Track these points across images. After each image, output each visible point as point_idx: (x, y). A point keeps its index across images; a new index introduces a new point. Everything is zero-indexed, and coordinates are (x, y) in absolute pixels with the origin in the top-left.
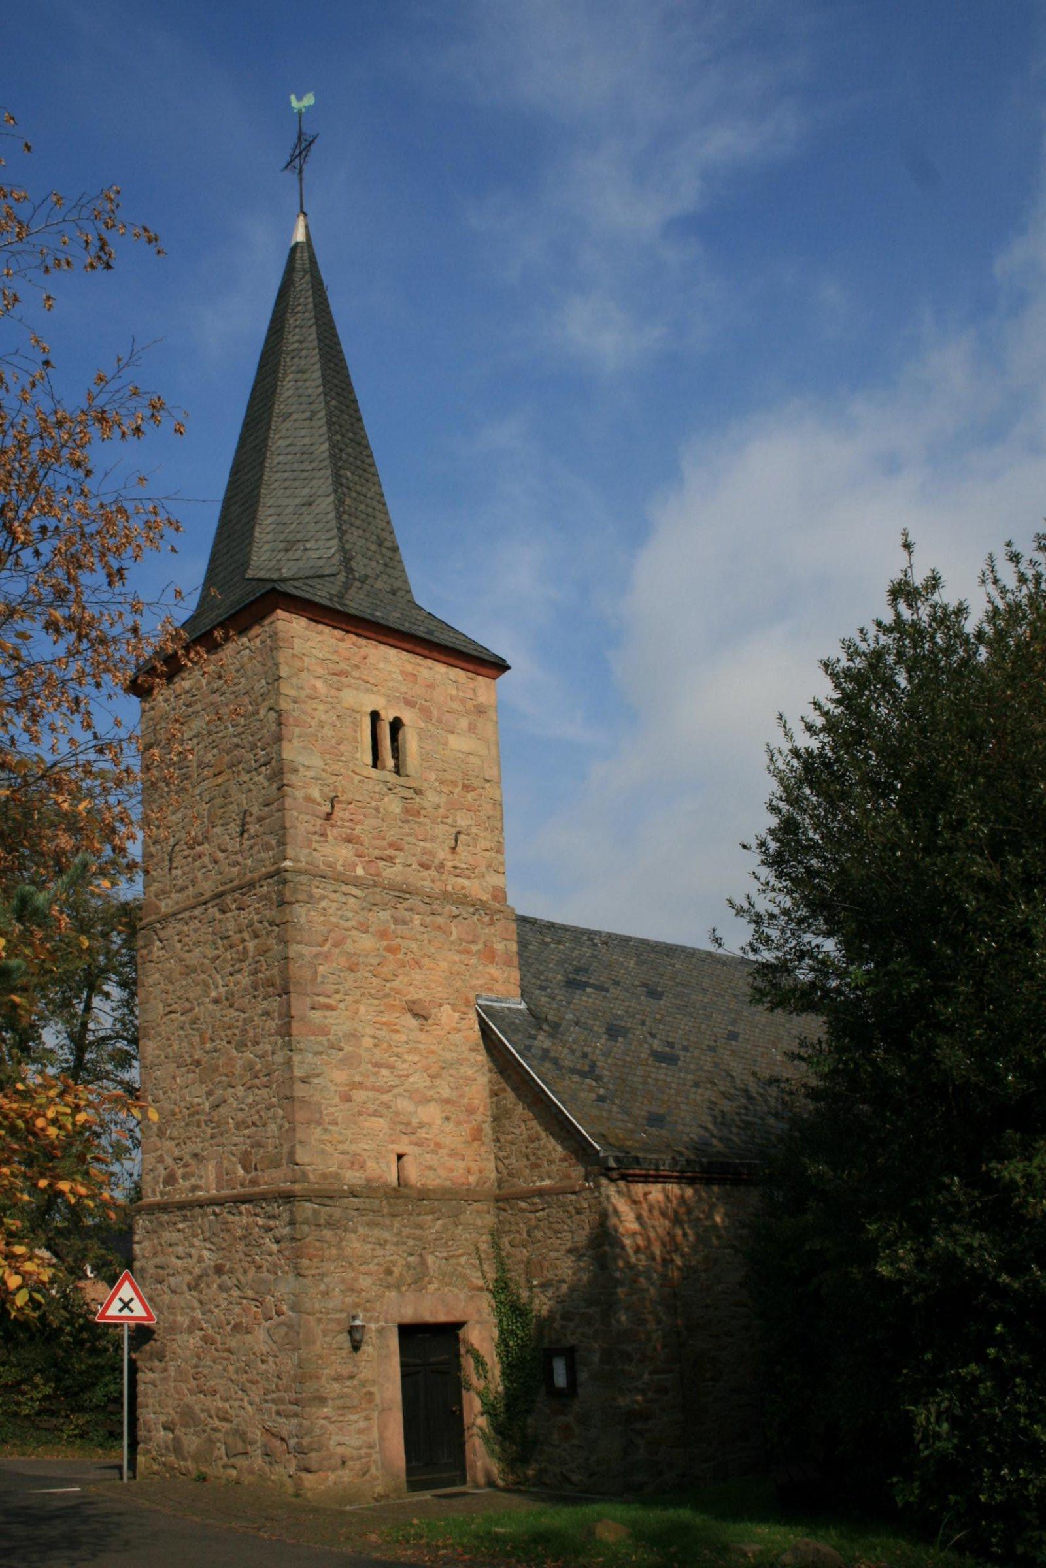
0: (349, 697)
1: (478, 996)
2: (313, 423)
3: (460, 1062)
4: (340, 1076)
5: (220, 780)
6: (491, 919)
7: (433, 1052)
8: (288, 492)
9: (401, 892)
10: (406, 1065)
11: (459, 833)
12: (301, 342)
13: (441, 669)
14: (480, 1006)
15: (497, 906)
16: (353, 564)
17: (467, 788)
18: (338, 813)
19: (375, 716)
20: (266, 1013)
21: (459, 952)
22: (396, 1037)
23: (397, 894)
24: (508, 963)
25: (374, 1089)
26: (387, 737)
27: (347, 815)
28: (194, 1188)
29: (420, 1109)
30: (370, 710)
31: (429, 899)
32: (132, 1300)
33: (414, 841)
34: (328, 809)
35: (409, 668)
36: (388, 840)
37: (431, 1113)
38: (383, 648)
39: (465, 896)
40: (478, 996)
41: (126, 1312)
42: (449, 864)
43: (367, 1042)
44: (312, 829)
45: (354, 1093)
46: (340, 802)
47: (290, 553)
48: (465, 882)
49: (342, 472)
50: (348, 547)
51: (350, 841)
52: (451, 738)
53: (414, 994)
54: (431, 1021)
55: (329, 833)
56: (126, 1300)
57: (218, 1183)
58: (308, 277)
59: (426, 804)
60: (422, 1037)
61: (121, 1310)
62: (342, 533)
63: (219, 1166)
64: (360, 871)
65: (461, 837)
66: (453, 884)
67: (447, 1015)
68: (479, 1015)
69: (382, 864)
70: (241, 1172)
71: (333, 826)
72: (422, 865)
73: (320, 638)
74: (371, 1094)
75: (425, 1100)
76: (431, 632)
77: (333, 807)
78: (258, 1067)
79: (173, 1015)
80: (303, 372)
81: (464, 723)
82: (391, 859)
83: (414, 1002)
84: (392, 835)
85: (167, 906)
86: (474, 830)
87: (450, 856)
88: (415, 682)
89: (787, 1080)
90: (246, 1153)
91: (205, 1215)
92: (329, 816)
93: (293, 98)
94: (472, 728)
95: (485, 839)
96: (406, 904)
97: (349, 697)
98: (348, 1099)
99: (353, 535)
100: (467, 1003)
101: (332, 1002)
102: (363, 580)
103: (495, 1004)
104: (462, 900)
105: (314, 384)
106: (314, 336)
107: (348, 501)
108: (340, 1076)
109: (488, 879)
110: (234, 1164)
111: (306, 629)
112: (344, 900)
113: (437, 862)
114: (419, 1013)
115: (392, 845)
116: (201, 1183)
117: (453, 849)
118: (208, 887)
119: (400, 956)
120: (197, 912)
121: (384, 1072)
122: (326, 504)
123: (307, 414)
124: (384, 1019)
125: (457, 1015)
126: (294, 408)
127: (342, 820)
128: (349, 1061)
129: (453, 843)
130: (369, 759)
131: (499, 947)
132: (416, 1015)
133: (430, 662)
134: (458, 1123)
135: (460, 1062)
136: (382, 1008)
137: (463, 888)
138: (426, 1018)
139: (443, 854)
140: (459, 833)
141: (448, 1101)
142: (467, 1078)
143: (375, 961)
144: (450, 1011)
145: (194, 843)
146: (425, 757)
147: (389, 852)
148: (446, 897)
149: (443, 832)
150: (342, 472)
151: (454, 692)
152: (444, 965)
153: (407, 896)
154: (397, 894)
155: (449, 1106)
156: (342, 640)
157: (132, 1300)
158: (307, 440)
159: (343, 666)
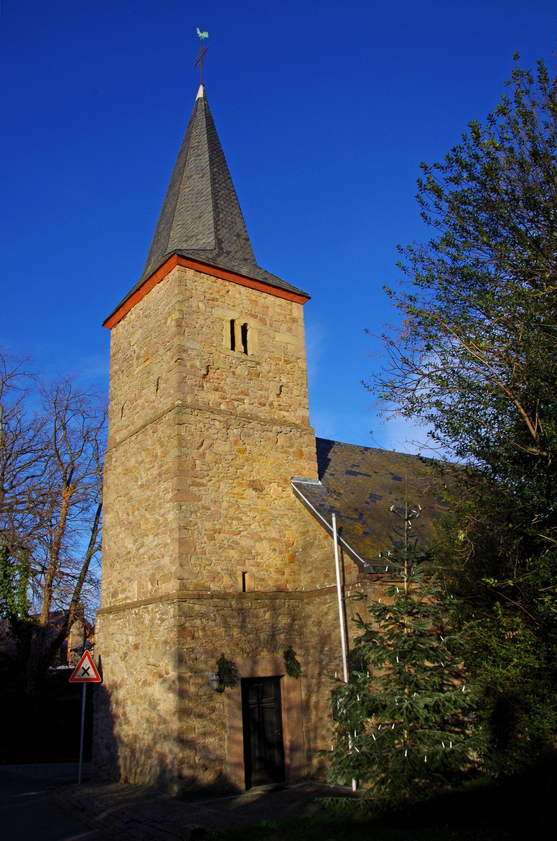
0: (218, 312)
1: (292, 478)
2: (204, 179)
3: (282, 516)
4: (208, 525)
5: (147, 363)
6: (301, 434)
7: (265, 511)
8: (189, 213)
9: (248, 418)
10: (248, 519)
11: (281, 386)
12: (199, 142)
13: (272, 298)
14: (294, 483)
15: (304, 427)
16: (223, 245)
17: (287, 362)
18: (211, 375)
19: (232, 322)
20: (166, 489)
21: (282, 453)
22: (243, 501)
23: (244, 419)
24: (310, 459)
25: (229, 532)
26: (240, 335)
27: (216, 376)
28: (127, 598)
29: (257, 544)
30: (230, 319)
31: (264, 422)
32: (89, 668)
33: (256, 390)
34: (204, 372)
35: (254, 298)
36: (240, 390)
37: (263, 547)
38: (238, 286)
39: (286, 421)
40: (292, 478)
41: (86, 676)
42: (276, 404)
43: (225, 504)
44: (194, 383)
45: (216, 535)
46: (212, 368)
47: (188, 242)
48: (284, 413)
49: (218, 201)
50: (219, 237)
51: (217, 390)
52: (277, 334)
53: (255, 476)
54: (264, 492)
55: (205, 385)
56: (86, 668)
57: (138, 595)
58: (203, 113)
59: (264, 371)
60: (259, 501)
61: (83, 675)
62: (217, 230)
63: (139, 584)
64: (223, 407)
65: (283, 389)
66: (278, 415)
67: (273, 489)
68: (294, 489)
69: (236, 403)
70: (150, 587)
71: (207, 381)
72: (260, 404)
73: (201, 281)
74: (228, 536)
75: (260, 539)
76: (266, 279)
77: (208, 371)
78: (161, 522)
79: (120, 498)
80: (199, 155)
81: (284, 327)
82: (242, 400)
83: (254, 481)
84: (242, 387)
85: (120, 437)
86: (291, 384)
87: (276, 399)
88: (257, 305)
89: (513, 133)
90: (154, 575)
91: (130, 614)
92: (205, 376)
93: (198, 30)
94: (290, 330)
95: (297, 390)
96: (250, 426)
97: (218, 312)
98: (212, 538)
99: (224, 232)
100: (286, 481)
101: (204, 481)
102: (228, 253)
103: (303, 482)
104: (284, 423)
105: (205, 161)
106: (206, 139)
107: (221, 216)
108: (208, 525)
109: (298, 411)
110: (147, 582)
111: (194, 276)
112: (212, 423)
113: (269, 402)
114: (257, 487)
115: (242, 393)
116: (129, 595)
117: (278, 395)
118: (139, 423)
119: (247, 455)
120: (133, 438)
121: (235, 522)
122: (209, 218)
123: (201, 175)
124: (235, 491)
125: (280, 488)
126: (194, 173)
127: (213, 378)
128: (214, 516)
129: (278, 392)
130: (229, 346)
131: (305, 450)
132: (255, 489)
133: (264, 295)
134: (281, 553)
135: (282, 516)
136: (235, 485)
137: (284, 417)
138: (261, 491)
139: (272, 397)
140: (281, 386)
141: (274, 540)
142: (287, 525)
143: (230, 457)
144: (276, 487)
145: (132, 401)
146: (262, 345)
147: (241, 396)
148: (274, 422)
149: (273, 388)
150: (218, 201)
151: (279, 311)
152: (272, 460)
153: (251, 421)
154: (244, 419)
155: (275, 543)
156: (215, 282)
157: (89, 668)
158: (200, 188)
159: (215, 295)
